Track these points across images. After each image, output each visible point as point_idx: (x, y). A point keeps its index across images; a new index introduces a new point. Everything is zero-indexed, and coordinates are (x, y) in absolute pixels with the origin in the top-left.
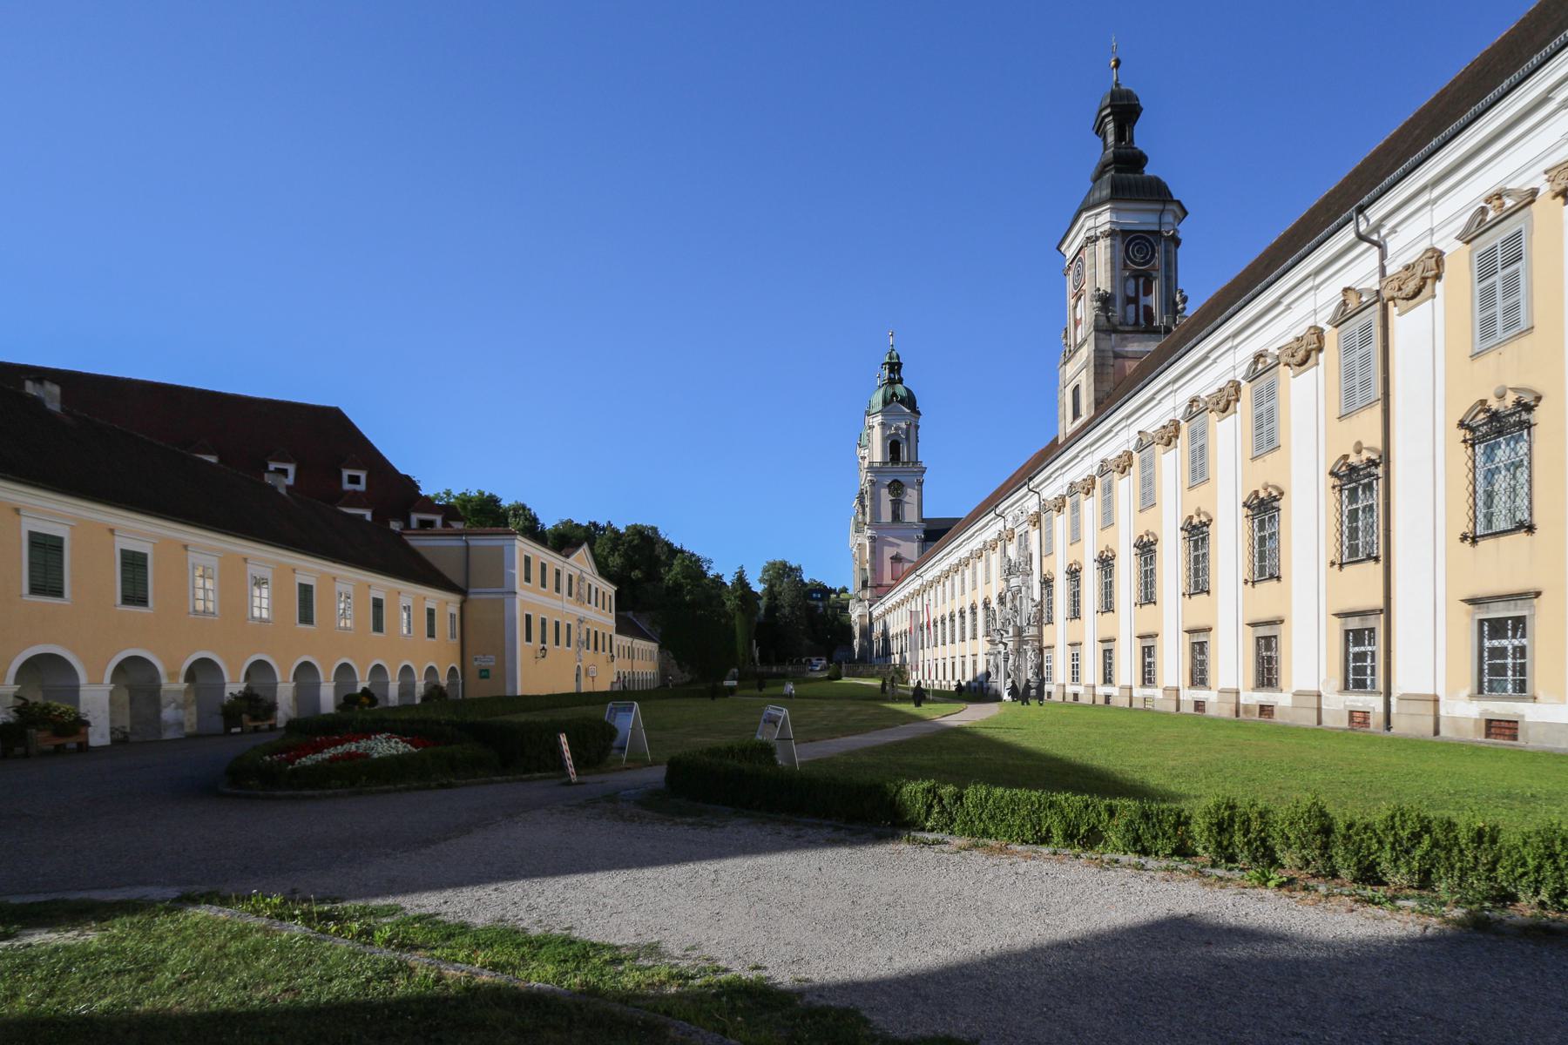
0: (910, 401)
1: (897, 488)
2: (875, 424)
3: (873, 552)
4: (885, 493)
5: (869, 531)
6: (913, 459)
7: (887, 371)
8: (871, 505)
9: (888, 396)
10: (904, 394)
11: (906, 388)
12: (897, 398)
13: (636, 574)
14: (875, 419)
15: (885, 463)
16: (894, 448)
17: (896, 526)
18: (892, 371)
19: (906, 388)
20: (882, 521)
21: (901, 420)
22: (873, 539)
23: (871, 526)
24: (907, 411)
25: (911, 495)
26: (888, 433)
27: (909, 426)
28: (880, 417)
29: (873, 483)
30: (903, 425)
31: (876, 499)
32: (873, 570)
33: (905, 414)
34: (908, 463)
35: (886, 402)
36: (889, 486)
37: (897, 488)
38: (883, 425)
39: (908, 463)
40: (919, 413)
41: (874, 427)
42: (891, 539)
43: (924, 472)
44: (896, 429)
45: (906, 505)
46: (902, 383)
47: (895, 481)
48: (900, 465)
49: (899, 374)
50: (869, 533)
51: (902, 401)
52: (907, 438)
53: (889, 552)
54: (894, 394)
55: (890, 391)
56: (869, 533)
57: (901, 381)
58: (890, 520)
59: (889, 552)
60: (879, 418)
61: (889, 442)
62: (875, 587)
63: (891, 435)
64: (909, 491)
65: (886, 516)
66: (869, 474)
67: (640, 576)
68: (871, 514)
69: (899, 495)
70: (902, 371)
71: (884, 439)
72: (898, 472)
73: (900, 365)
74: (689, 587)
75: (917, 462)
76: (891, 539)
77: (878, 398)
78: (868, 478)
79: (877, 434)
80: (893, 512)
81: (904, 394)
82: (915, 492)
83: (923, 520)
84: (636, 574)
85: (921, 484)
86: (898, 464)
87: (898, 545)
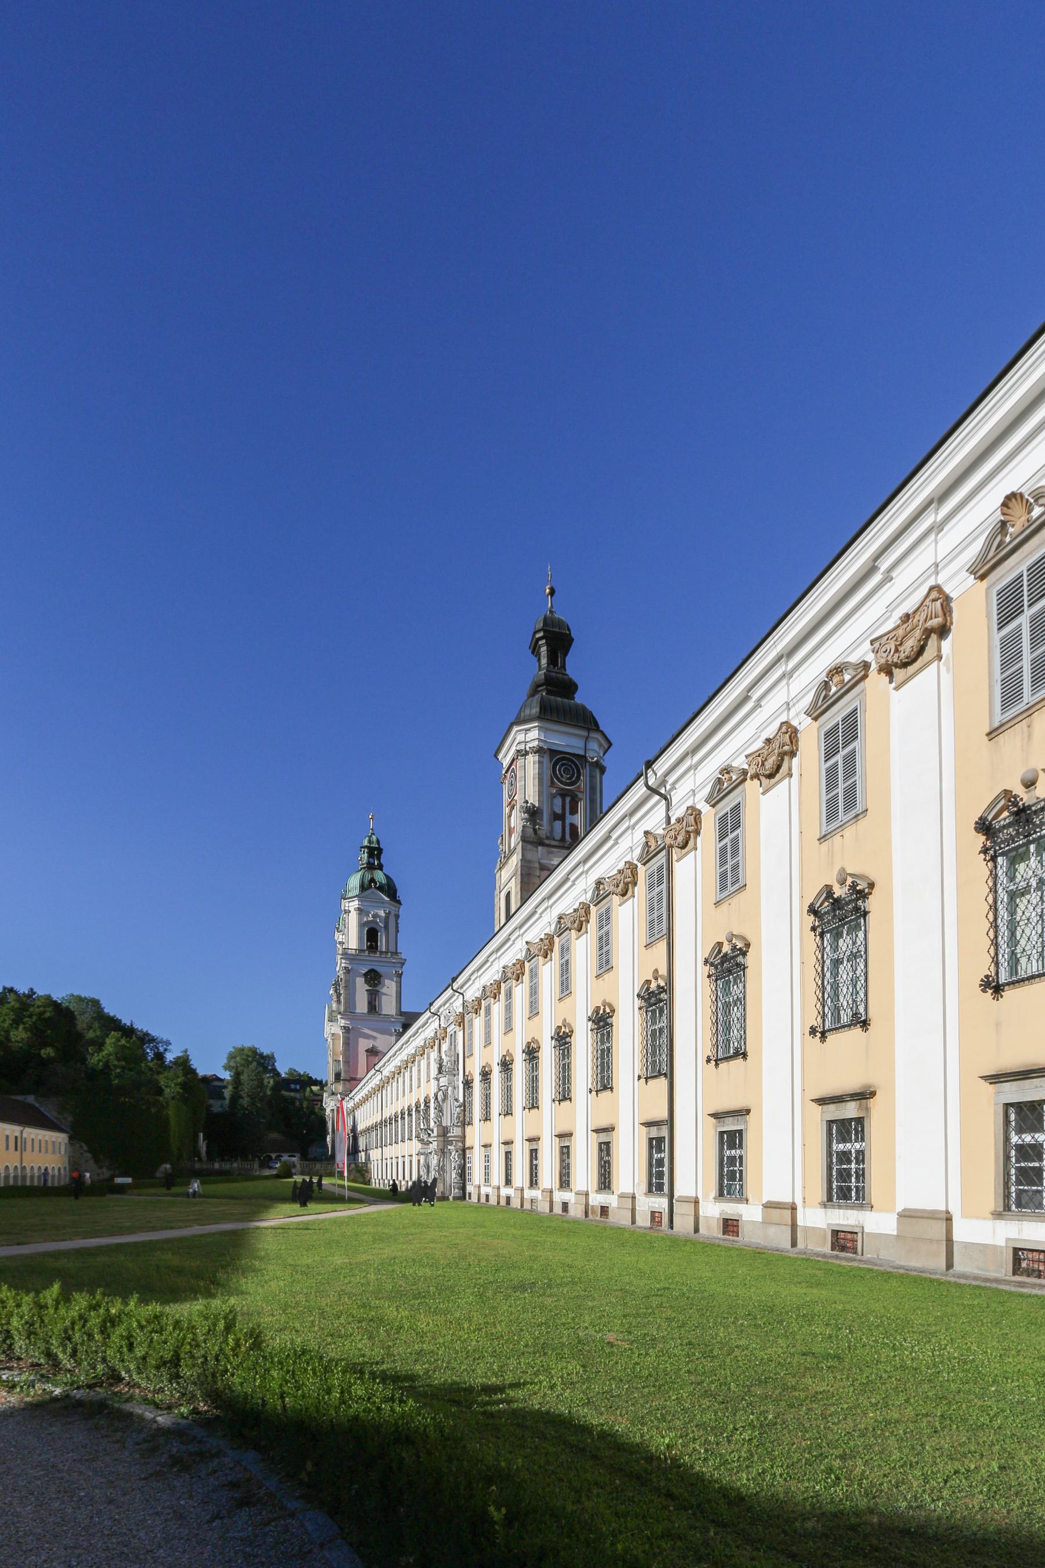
0: (390, 890)
1: (373, 978)
2: (352, 909)
3: (347, 1043)
4: (360, 981)
5: (343, 1021)
6: (392, 949)
7: (366, 855)
8: (346, 994)
9: (366, 881)
10: (384, 881)
11: (387, 877)
12: (376, 884)
13: (48, 1052)
14: (351, 904)
15: (361, 951)
16: (371, 935)
17: (372, 1017)
18: (371, 855)
19: (387, 877)
20: (357, 1011)
21: (379, 908)
22: (346, 1030)
23: (344, 1015)
24: (387, 899)
25: (389, 987)
26: (365, 920)
27: (388, 915)
28: (357, 902)
29: (347, 971)
30: (382, 913)
31: (350, 987)
32: (347, 1062)
33: (384, 902)
34: (386, 952)
35: (363, 888)
36: (365, 975)
37: (373, 978)
38: (360, 911)
39: (386, 952)
40: (399, 902)
41: (350, 912)
42: (366, 1031)
43: (403, 964)
44: (373, 916)
45: (383, 997)
46: (382, 870)
47: (372, 971)
48: (378, 954)
49: (379, 859)
50: (342, 1022)
51: (381, 888)
52: (386, 927)
53: (364, 1044)
54: (372, 880)
55: (368, 877)
56: (342, 1022)
57: (380, 867)
58: (365, 1011)
59: (364, 1044)
60: (355, 904)
61: (366, 929)
62: (349, 1081)
63: (368, 922)
64: (387, 982)
65: (362, 1006)
66: (343, 961)
67: (52, 1054)
68: (345, 1003)
69: (376, 985)
70: (382, 856)
71: (361, 925)
72: (374, 962)
73: (380, 850)
74: (118, 1070)
75: (396, 953)
76: (366, 1031)
77: (354, 882)
78: (343, 965)
79: (353, 920)
80: (369, 1003)
81: (384, 881)
82: (394, 984)
83: (401, 1014)
84: (48, 1052)
85: (400, 976)
86: (375, 952)
87: (375, 1038)
